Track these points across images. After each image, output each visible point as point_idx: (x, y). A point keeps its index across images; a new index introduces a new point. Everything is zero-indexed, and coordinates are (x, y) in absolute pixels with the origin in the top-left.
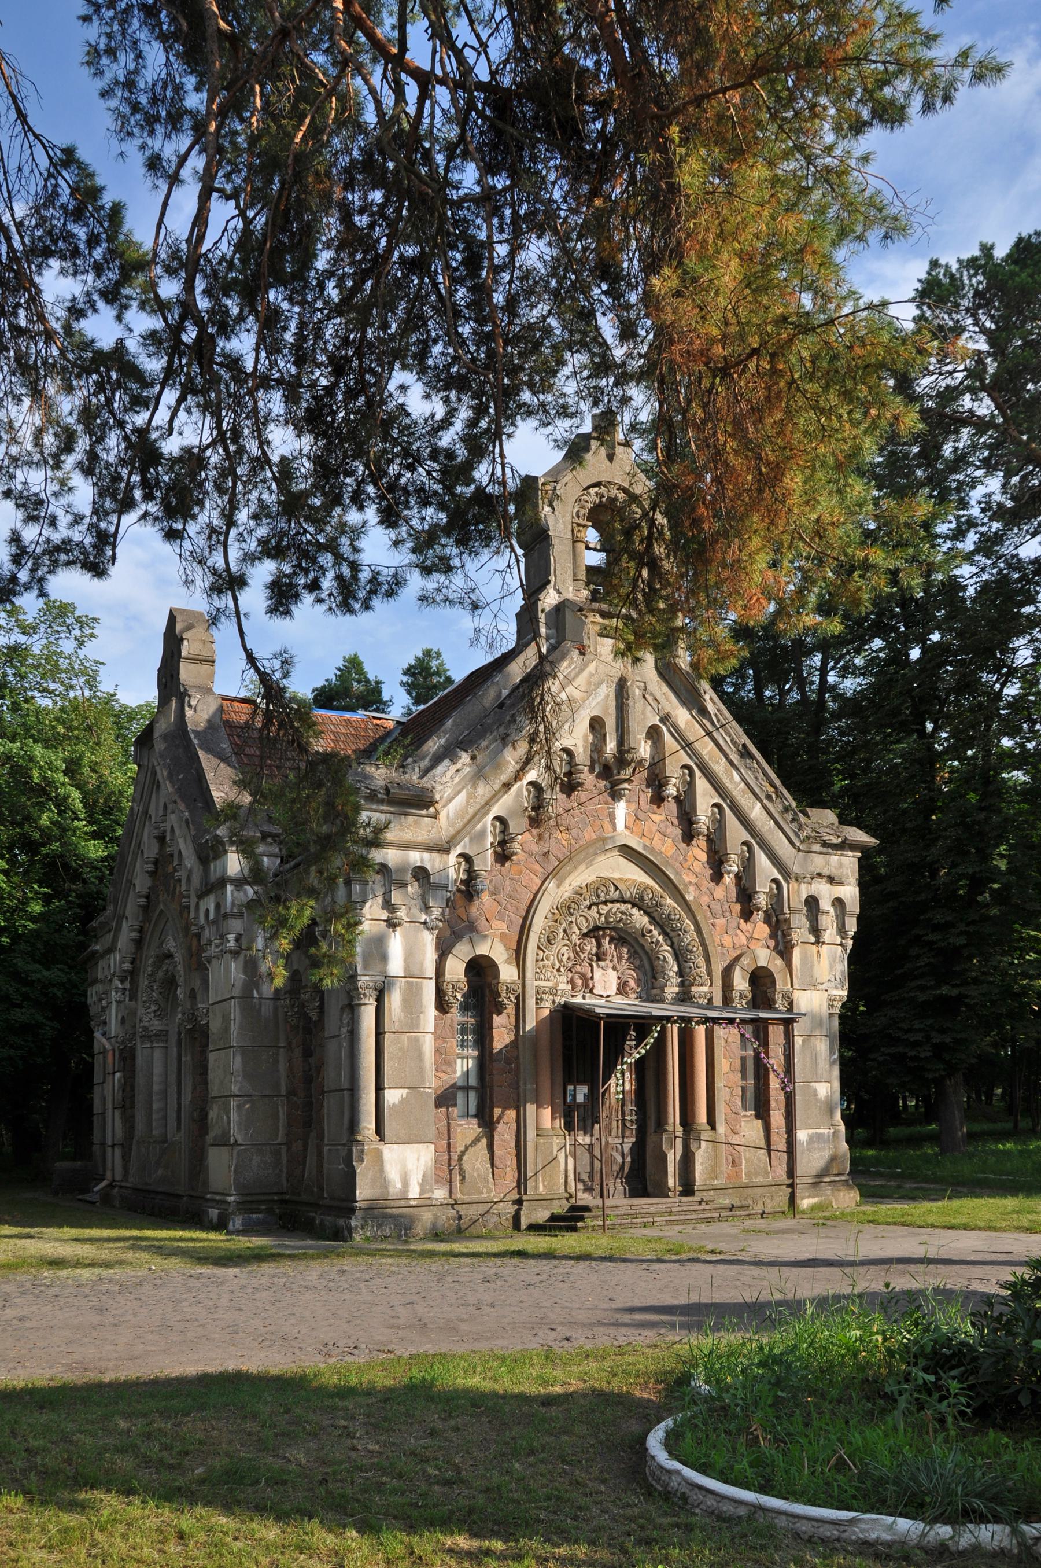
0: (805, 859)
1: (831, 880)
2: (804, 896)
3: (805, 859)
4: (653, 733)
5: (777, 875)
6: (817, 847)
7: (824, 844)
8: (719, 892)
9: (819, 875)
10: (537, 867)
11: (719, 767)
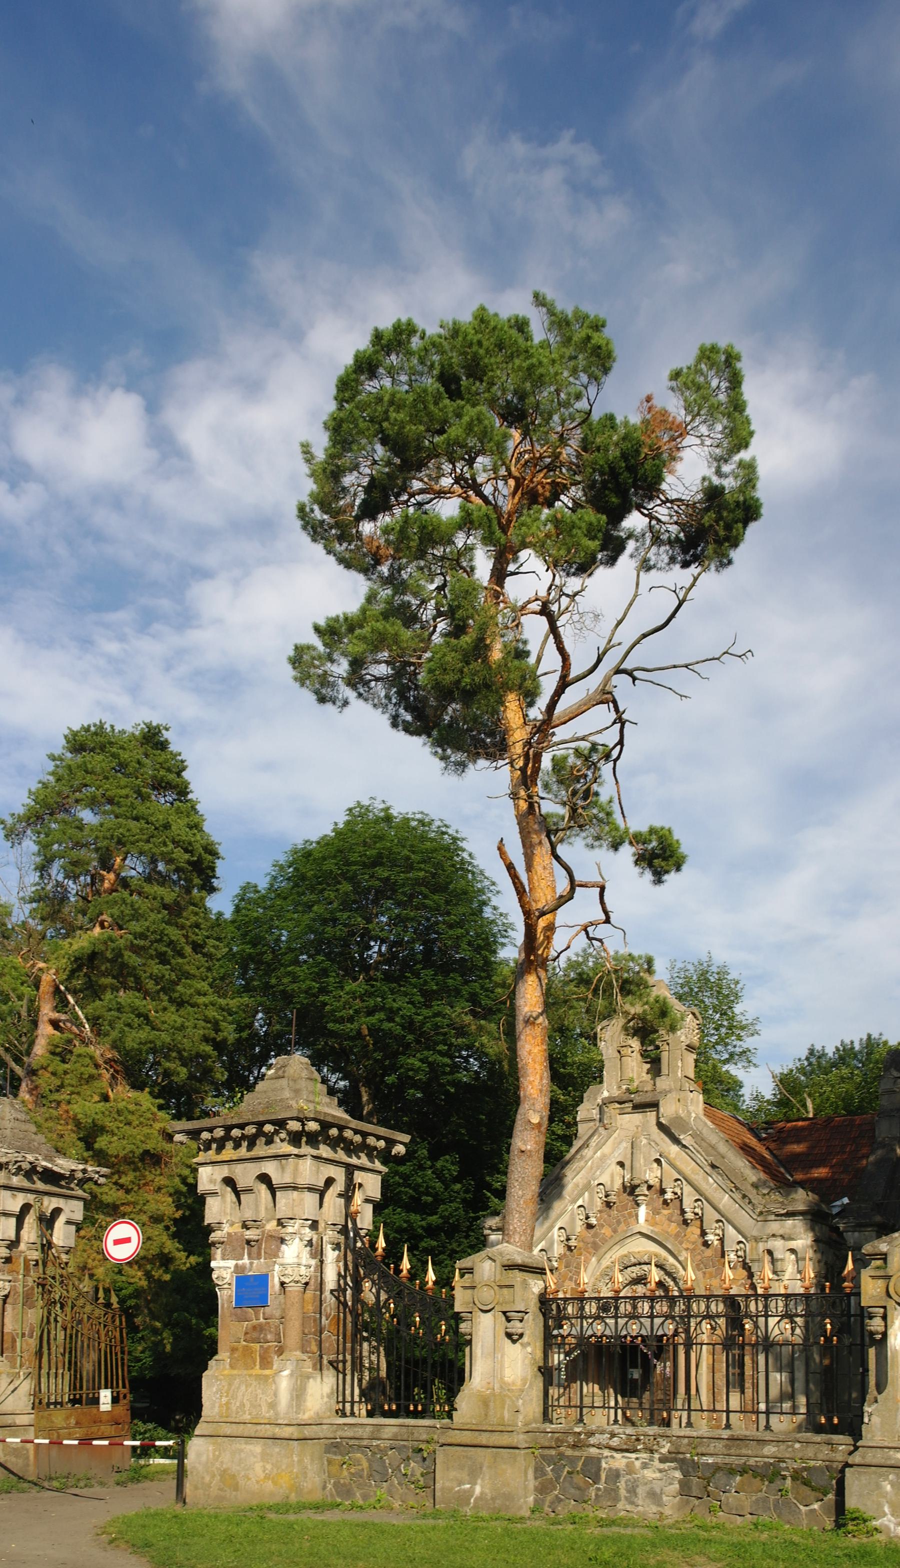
0: (763, 1226)
1: (782, 1237)
2: (761, 1250)
3: (763, 1226)
4: (658, 1161)
5: (741, 1238)
6: (773, 1217)
7: (777, 1215)
8: (709, 1252)
9: (774, 1235)
10: (591, 1250)
11: (698, 1177)
